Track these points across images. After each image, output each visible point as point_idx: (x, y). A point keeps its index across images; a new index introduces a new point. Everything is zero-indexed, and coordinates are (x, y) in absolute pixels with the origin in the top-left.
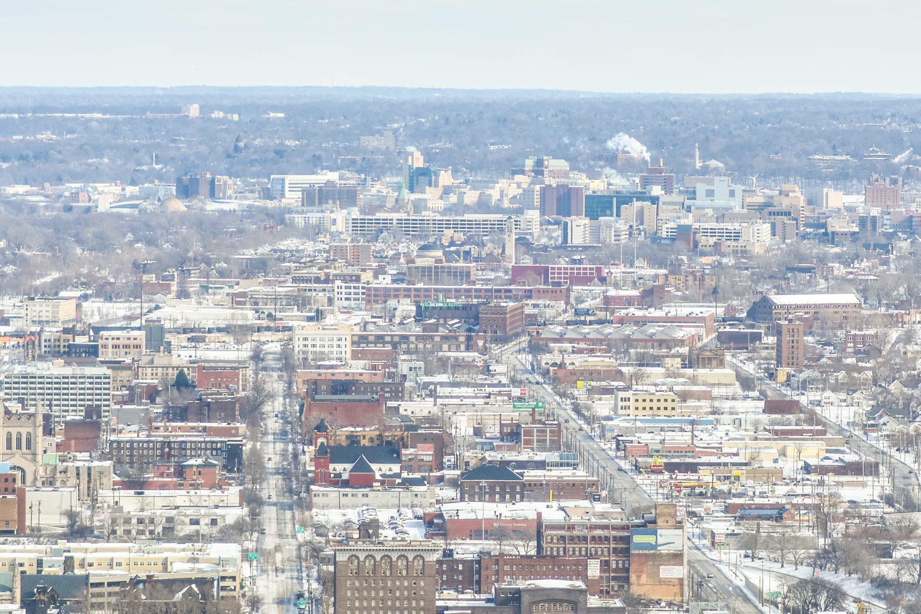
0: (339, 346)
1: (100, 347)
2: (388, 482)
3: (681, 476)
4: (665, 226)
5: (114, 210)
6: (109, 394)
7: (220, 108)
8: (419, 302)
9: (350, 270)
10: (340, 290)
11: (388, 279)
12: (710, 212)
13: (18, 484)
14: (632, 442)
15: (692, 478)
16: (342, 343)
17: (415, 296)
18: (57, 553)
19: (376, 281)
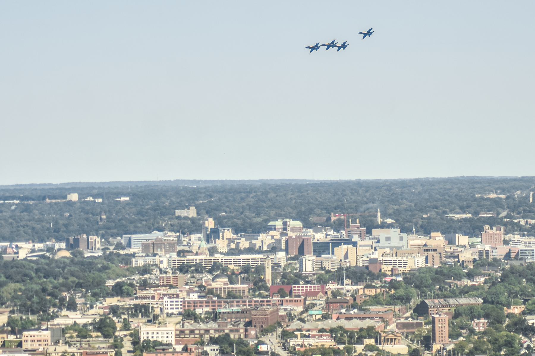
1: (23, 342)
7: (91, 196)
8: (215, 309)
10: (167, 303)
16: (170, 335)
19: (188, 297)
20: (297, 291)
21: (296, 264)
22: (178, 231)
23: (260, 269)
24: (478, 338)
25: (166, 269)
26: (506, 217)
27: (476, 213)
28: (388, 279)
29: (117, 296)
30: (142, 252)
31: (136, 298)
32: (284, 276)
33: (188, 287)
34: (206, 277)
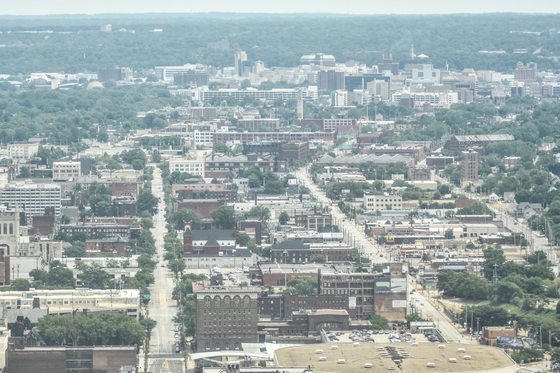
0: (197, 169)
2: (228, 252)
3: (405, 246)
4: (393, 95)
5: (61, 89)
6: (59, 200)
7: (124, 27)
8: (246, 142)
9: (203, 124)
10: (197, 136)
11: (227, 128)
12: (420, 86)
13: (6, 255)
14: (374, 225)
15: (411, 247)
16: (199, 168)
17: (243, 139)
18: (29, 296)
20: (328, 125)
21: (328, 98)
22: (211, 64)
23: (292, 104)
24: (508, 175)
25: (198, 101)
26: (540, 54)
27: (510, 50)
28: (420, 115)
29: (148, 128)
30: (175, 84)
31: (168, 130)
32: (316, 111)
33: (219, 120)
34: (237, 110)
